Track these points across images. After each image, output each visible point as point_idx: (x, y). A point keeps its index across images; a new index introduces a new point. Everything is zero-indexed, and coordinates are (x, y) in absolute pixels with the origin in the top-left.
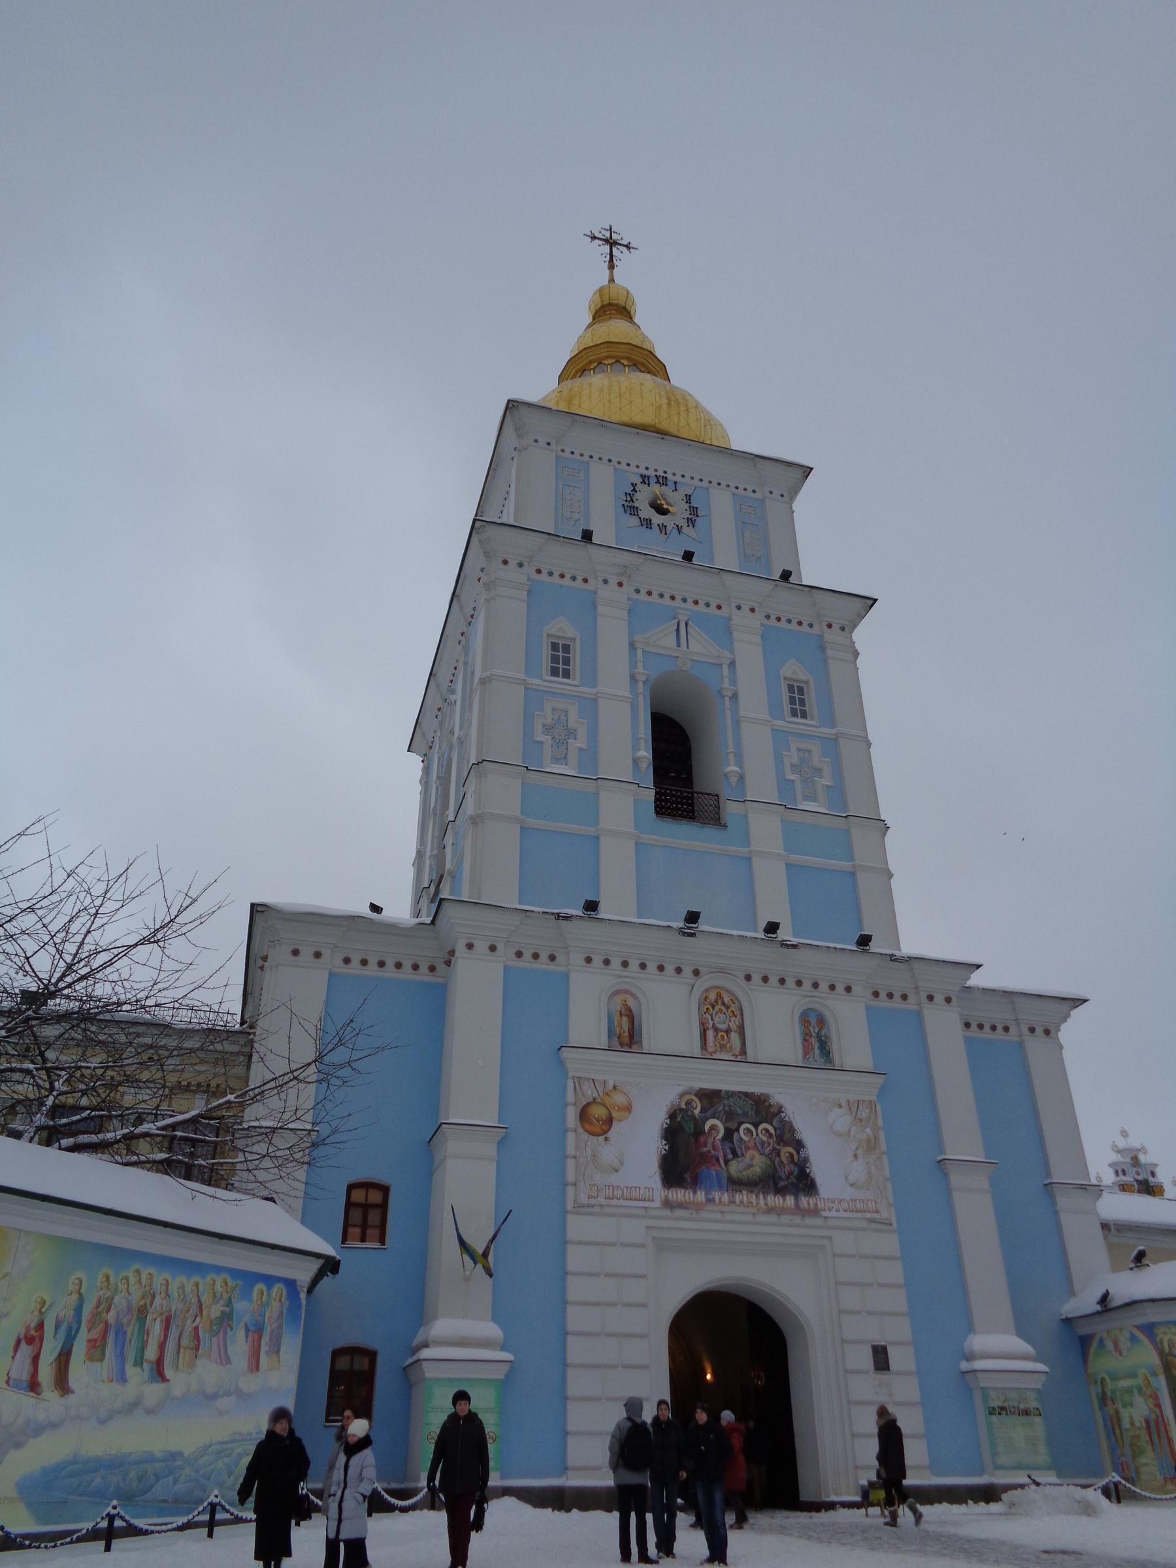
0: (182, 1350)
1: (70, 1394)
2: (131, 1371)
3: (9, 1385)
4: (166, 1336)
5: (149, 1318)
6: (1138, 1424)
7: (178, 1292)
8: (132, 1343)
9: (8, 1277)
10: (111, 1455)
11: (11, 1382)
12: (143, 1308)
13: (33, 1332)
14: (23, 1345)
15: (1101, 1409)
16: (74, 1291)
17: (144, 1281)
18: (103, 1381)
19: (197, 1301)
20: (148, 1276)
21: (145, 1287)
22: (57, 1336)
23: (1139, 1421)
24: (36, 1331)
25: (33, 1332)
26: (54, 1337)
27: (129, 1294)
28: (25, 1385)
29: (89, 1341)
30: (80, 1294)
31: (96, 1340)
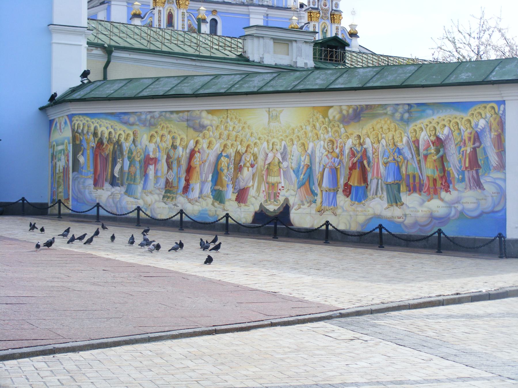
6: (61, 171)
15: (52, 162)
23: (61, 168)
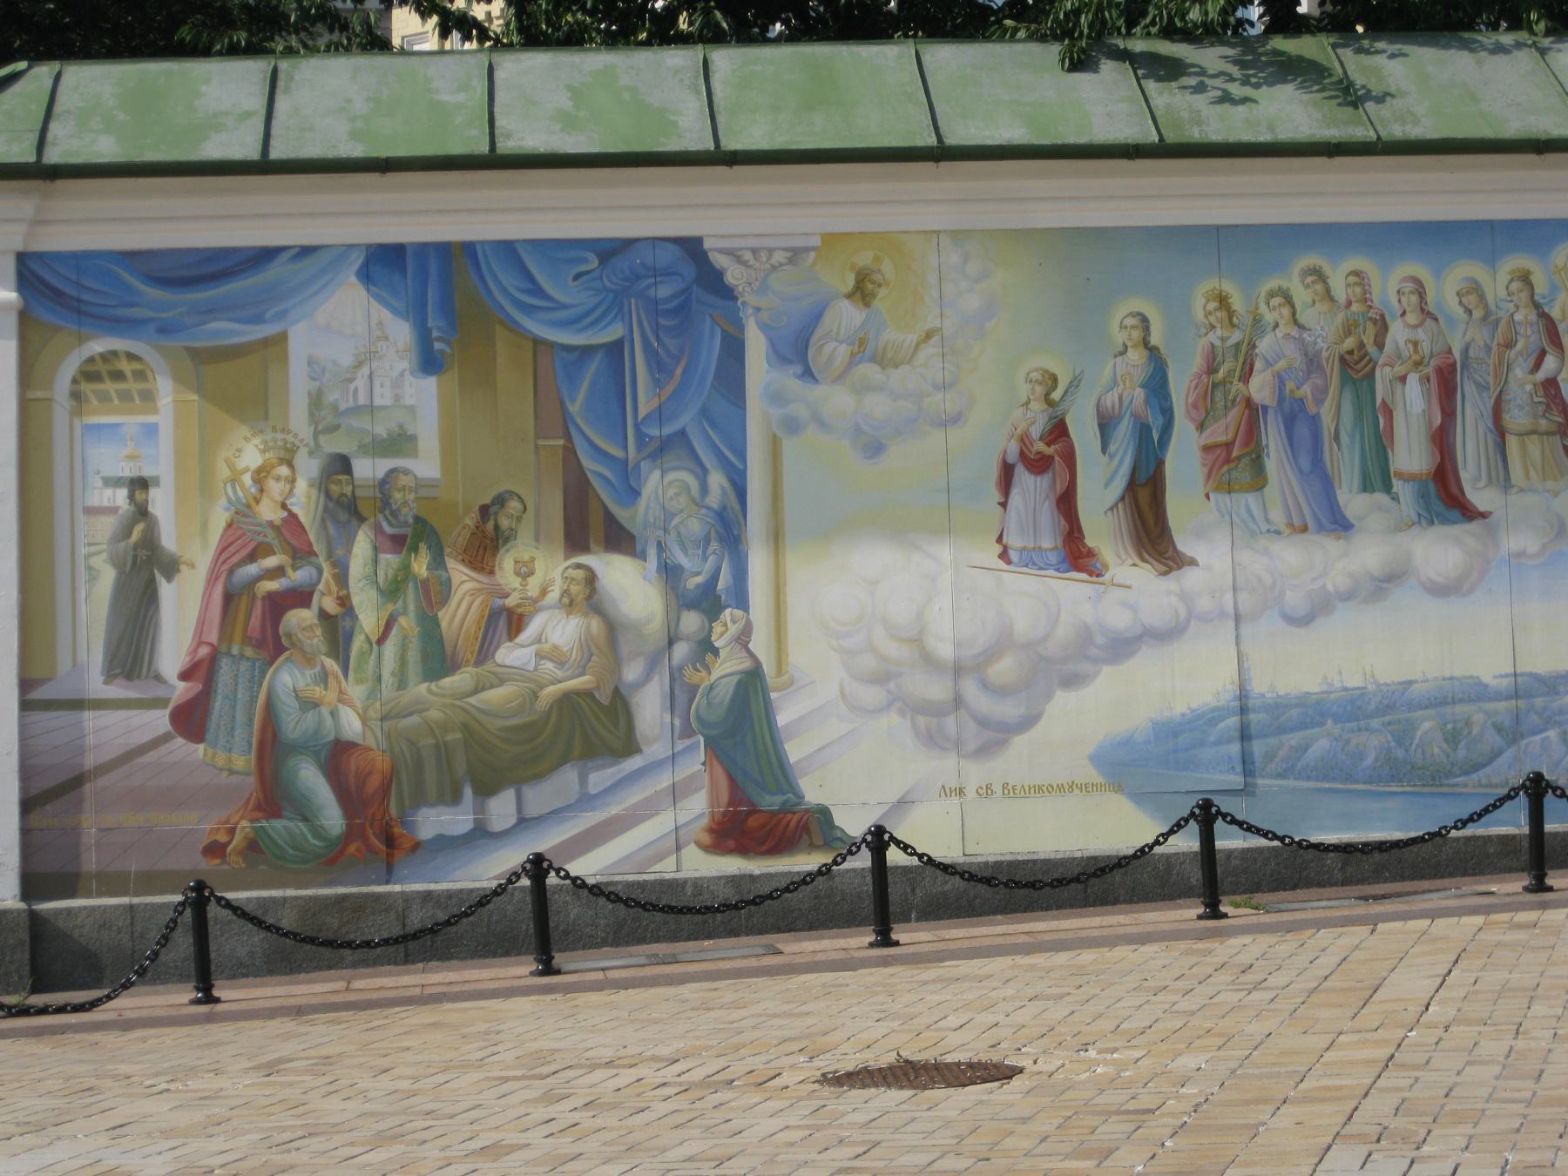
0: (1512, 443)
1: (1186, 568)
2: (1353, 502)
3: (1009, 562)
4: (1449, 413)
5: (1382, 376)
7: (1461, 303)
8: (1344, 438)
9: (936, 338)
10: (1345, 689)
11: (1013, 555)
12: (1356, 357)
13: (1041, 447)
14: (1022, 476)
16: (1129, 344)
17: (1340, 293)
18: (1278, 533)
19: (1533, 316)
20: (1352, 279)
21: (1349, 304)
22: (1112, 448)
24: (1049, 444)
25: (1041, 447)
26: (1104, 450)
27: (1301, 327)
28: (1053, 558)
29: (1207, 449)
30: (1152, 351)
31: (1229, 446)
